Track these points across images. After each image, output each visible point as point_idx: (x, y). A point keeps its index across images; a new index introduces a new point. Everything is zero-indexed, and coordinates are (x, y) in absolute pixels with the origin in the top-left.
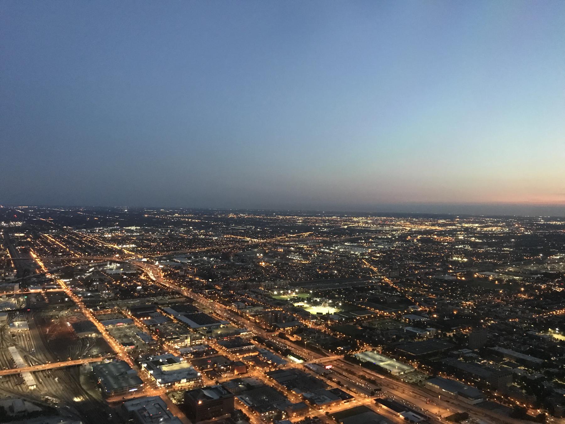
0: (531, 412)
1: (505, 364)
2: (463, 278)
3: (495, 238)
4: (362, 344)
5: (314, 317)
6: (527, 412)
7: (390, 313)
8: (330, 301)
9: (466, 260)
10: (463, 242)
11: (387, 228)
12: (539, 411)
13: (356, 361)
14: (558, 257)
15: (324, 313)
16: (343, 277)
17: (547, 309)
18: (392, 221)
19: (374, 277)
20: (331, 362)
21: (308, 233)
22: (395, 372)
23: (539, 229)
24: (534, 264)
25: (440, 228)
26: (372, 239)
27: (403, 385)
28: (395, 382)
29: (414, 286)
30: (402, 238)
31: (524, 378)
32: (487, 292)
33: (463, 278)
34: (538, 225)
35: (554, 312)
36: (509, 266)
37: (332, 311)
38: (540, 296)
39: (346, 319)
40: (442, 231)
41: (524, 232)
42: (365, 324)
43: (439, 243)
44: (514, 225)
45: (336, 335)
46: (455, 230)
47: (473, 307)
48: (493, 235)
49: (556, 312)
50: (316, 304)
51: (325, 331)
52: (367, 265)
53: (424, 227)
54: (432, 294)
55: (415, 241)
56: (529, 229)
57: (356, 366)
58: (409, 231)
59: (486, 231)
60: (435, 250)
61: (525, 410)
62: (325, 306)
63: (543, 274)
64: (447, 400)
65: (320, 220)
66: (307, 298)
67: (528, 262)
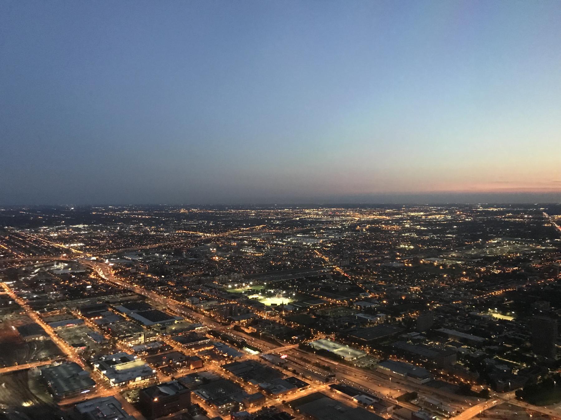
0: (475, 388)
1: (450, 344)
2: (410, 265)
3: (440, 225)
4: (316, 333)
5: (268, 308)
6: (470, 388)
7: (342, 301)
8: (284, 292)
9: (412, 247)
10: (409, 230)
11: (337, 219)
13: (310, 349)
14: (496, 242)
15: (278, 304)
16: (296, 267)
17: (487, 291)
18: (341, 212)
19: (326, 266)
20: (286, 351)
21: (261, 226)
22: (348, 358)
25: (388, 218)
26: (323, 229)
27: (356, 370)
28: (348, 367)
29: (364, 274)
30: (352, 228)
31: (467, 356)
32: (433, 277)
33: (410, 265)
36: (452, 251)
37: (286, 301)
38: (481, 278)
39: (300, 308)
40: (389, 220)
42: (318, 312)
43: (386, 232)
44: (456, 212)
45: (291, 325)
46: (401, 219)
47: (420, 292)
48: (436, 223)
49: (495, 293)
50: (270, 295)
51: (280, 322)
52: (318, 255)
53: (372, 217)
54: (382, 281)
55: (364, 230)
56: (469, 216)
57: (310, 354)
58: (358, 221)
59: (431, 219)
60: (383, 239)
61: (468, 387)
62: (279, 297)
63: (483, 257)
64: (398, 381)
65: (273, 213)
66: (261, 290)
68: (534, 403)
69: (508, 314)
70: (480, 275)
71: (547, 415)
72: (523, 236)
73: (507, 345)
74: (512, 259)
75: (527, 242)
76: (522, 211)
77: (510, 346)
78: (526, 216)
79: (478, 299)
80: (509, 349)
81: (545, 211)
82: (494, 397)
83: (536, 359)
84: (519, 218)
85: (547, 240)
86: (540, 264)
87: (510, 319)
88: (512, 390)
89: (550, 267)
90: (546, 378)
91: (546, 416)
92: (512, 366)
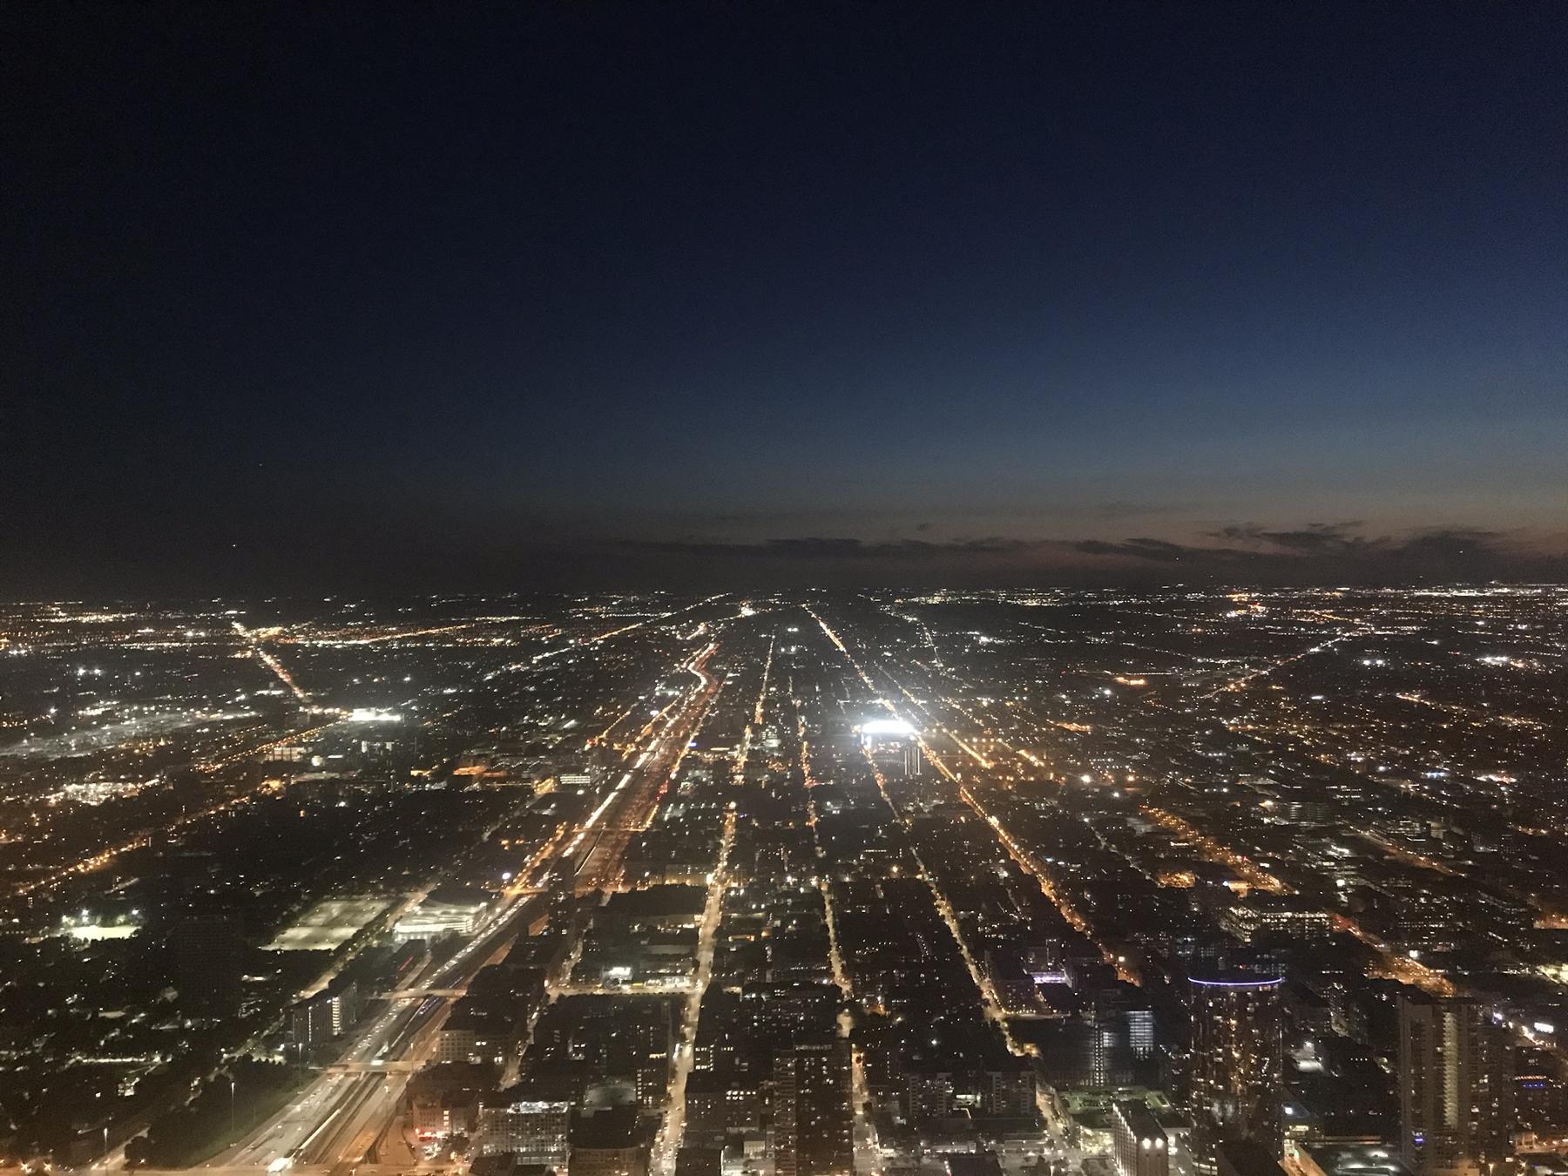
12: (24, 1166)
14: (99, 712)
23: (50, 639)
24: (29, 738)
34: (48, 626)
35: (80, 867)
41: (7, 649)
56: (23, 640)
67: (16, 735)
69: (121, 919)
72: (179, 687)
73: (110, 1015)
74: (144, 756)
75: (186, 706)
77: (119, 1014)
78: (190, 634)
79: (30, 893)
80: (114, 1023)
81: (238, 619)
85: (238, 694)
86: (215, 763)
87: (125, 932)
88: (112, 1146)
89: (241, 767)
90: (212, 1078)
92: (113, 1076)
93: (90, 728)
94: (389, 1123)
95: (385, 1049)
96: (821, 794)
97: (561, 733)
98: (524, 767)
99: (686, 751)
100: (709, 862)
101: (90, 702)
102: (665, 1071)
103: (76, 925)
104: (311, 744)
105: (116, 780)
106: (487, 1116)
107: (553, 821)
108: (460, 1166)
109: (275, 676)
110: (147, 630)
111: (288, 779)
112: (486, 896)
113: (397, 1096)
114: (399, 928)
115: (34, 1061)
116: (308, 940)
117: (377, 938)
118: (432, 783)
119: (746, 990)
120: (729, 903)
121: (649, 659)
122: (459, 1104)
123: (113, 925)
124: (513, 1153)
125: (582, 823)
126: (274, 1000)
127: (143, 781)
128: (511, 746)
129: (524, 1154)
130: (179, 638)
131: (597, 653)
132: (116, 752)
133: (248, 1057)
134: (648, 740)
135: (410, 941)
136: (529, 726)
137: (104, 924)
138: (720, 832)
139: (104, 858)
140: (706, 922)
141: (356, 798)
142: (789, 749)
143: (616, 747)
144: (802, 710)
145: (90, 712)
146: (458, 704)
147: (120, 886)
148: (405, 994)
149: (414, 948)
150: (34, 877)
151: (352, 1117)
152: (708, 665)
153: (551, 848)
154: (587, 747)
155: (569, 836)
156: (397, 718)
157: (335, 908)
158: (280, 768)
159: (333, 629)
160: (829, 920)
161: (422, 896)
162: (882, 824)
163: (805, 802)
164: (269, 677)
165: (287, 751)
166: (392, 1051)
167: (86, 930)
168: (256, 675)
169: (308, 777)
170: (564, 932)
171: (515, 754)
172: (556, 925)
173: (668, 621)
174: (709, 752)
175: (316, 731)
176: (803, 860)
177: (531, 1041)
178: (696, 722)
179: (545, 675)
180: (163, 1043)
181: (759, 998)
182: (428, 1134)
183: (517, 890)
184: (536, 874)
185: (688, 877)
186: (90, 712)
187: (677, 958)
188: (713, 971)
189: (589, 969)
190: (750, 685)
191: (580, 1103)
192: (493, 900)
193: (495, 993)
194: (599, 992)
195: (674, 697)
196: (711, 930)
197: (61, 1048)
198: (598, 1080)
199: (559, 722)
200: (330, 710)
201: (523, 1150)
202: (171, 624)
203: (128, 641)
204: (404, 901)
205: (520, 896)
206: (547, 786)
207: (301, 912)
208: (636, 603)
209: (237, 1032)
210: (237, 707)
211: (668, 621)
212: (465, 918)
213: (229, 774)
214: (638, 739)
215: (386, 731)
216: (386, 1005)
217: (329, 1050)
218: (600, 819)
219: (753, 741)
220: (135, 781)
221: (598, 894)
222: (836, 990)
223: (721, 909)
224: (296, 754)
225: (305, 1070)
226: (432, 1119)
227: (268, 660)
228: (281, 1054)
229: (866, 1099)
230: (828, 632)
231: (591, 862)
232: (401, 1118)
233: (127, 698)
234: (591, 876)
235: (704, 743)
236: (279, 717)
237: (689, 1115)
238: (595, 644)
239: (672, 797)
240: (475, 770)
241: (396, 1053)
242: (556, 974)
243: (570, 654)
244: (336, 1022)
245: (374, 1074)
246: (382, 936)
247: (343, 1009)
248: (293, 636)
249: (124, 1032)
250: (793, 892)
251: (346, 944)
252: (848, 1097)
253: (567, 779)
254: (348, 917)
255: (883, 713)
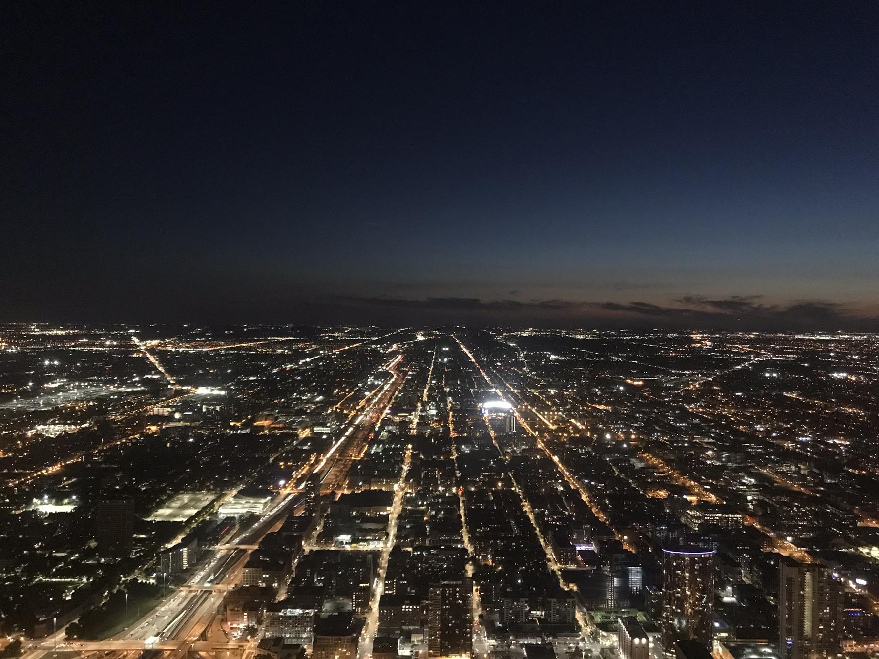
12: (9, 638)
14: (56, 385)
24: (17, 399)
34: (29, 337)
35: (44, 471)
38: (24, 449)
41: (5, 349)
56: (15, 344)
67: (9, 397)
68: (93, 638)
69: (66, 501)
70: (24, 444)
71: (114, 651)
72: (100, 372)
73: (59, 555)
74: (81, 411)
75: (106, 383)
76: (101, 336)
78: (108, 343)
79: (16, 486)
81: (135, 335)
82: (30, 649)
83: (102, 564)
84: (97, 346)
87: (68, 509)
88: (59, 627)
89: (134, 418)
90: (115, 591)
91: (113, 653)
92: (60, 588)
93: (52, 394)
94: (214, 619)
95: (212, 577)
96: (459, 441)
97: (314, 403)
98: (294, 422)
99: (384, 416)
100: (395, 476)
101: (51, 379)
102: (368, 594)
103: (41, 504)
104: (174, 406)
105: (65, 424)
106: (268, 616)
107: (309, 453)
108: (252, 645)
109: (156, 368)
110: (85, 340)
111: (161, 425)
112: (270, 493)
113: (218, 604)
114: (221, 510)
115: (16, 579)
116: (170, 515)
117: (209, 515)
118: (242, 429)
119: (415, 550)
120: (406, 501)
121: (365, 363)
122: (251, 608)
123: (62, 505)
124: (282, 637)
125: (325, 454)
126: (151, 548)
127: (80, 424)
128: (286, 410)
129: (288, 638)
130: (101, 345)
131: (336, 359)
132: (65, 408)
133: (135, 580)
134: (363, 408)
135: (227, 518)
136: (296, 399)
137: (57, 504)
138: (402, 462)
139: (57, 467)
140: (393, 511)
141: (199, 437)
142: (442, 416)
143: (345, 412)
144: (450, 394)
145: (51, 385)
146: (257, 386)
147: (66, 483)
148: (224, 547)
149: (230, 520)
150: (17, 476)
151: (193, 615)
152: (399, 366)
153: (308, 467)
154: (329, 411)
155: (318, 461)
156: (223, 393)
157: (186, 498)
158: (156, 419)
159: (188, 342)
160: (462, 512)
161: (235, 492)
162: (493, 459)
163: (450, 445)
164: (152, 368)
165: (161, 410)
166: (216, 578)
167: (46, 507)
168: (143, 367)
169: (172, 424)
170: (314, 514)
171: (289, 415)
172: (309, 510)
173: (375, 342)
174: (397, 416)
175: (178, 399)
176: (448, 476)
177: (294, 575)
178: (391, 398)
179: (306, 371)
180: (88, 571)
181: (422, 554)
182: (235, 626)
183: (287, 491)
184: (299, 482)
185: (384, 485)
186: (51, 385)
187: (377, 530)
188: (396, 538)
189: (328, 535)
190: (421, 379)
191: (320, 611)
192: (274, 495)
193: (273, 548)
194: (333, 549)
195: (378, 385)
196: (396, 516)
197: (30, 573)
198: (330, 598)
199: (314, 397)
200: (185, 388)
201: (288, 635)
202: (98, 337)
203: (73, 346)
204: (225, 495)
205: (289, 494)
206: (305, 433)
207: (167, 500)
208: (358, 332)
209: (129, 566)
210: (133, 384)
211: (375, 342)
212: (258, 505)
213: (129, 422)
214: (358, 408)
215: (216, 399)
216: (213, 553)
217: (181, 578)
218: (334, 452)
219: (422, 411)
220: (76, 424)
221: (333, 494)
222: (465, 550)
223: (402, 504)
224: (166, 411)
225: (167, 588)
226: (237, 616)
227: (152, 359)
228: (154, 578)
229: (480, 613)
230: (465, 350)
231: (330, 476)
232: (220, 616)
233: (72, 378)
234: (328, 484)
235: (395, 411)
236: (157, 390)
237: (381, 618)
238: (334, 354)
239: (376, 441)
240: (266, 423)
241: (217, 580)
242: (308, 538)
243: (321, 359)
244: (185, 562)
245: (205, 591)
246: (211, 514)
247: (190, 555)
248: (166, 346)
249: (67, 564)
250: (442, 496)
251: (192, 518)
252: (470, 611)
253: (317, 429)
254: (193, 503)
255: (495, 397)
